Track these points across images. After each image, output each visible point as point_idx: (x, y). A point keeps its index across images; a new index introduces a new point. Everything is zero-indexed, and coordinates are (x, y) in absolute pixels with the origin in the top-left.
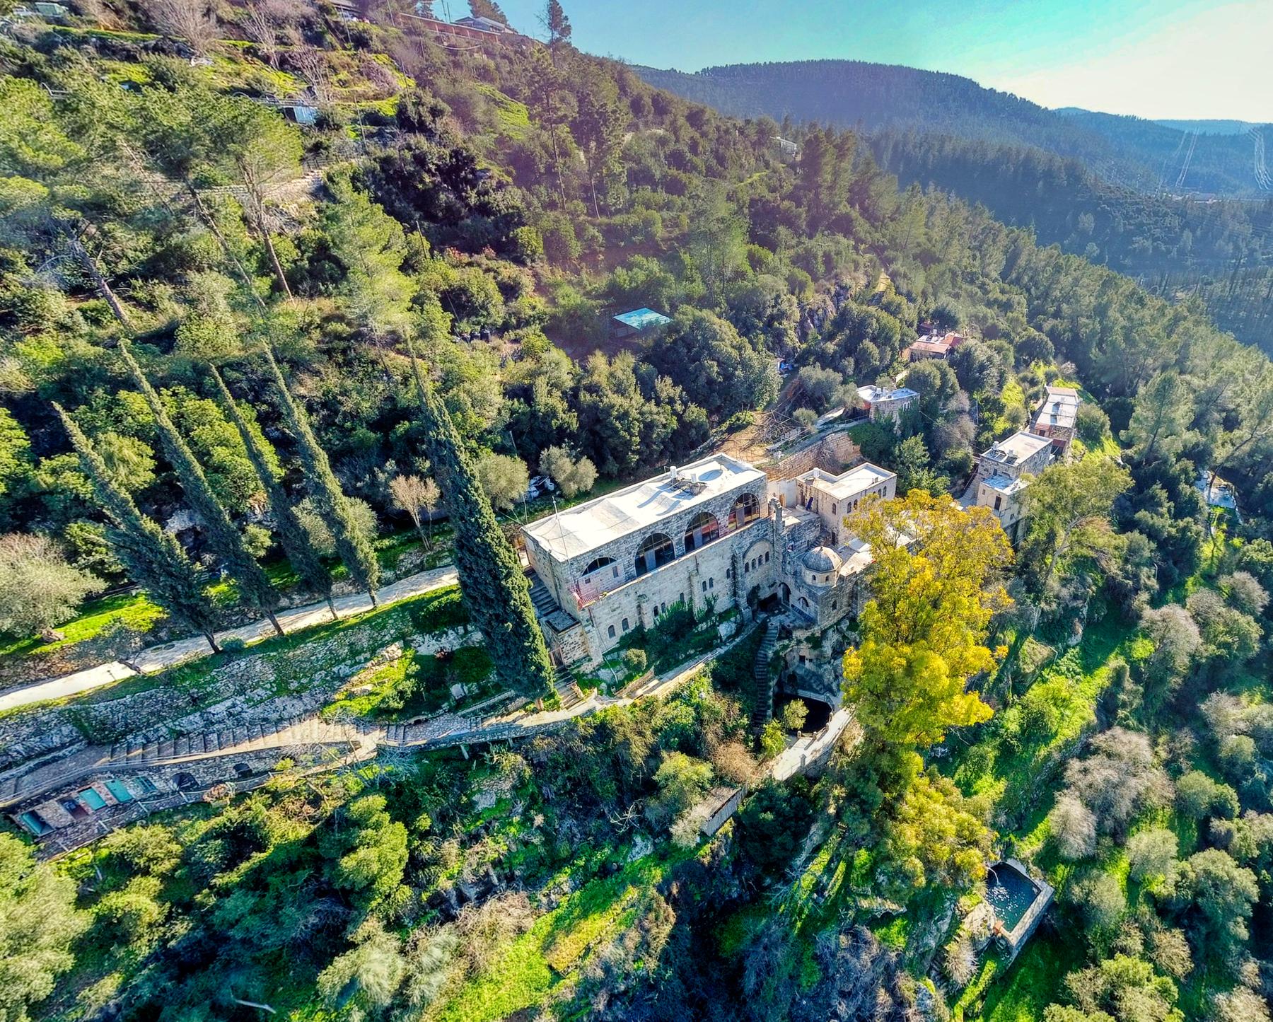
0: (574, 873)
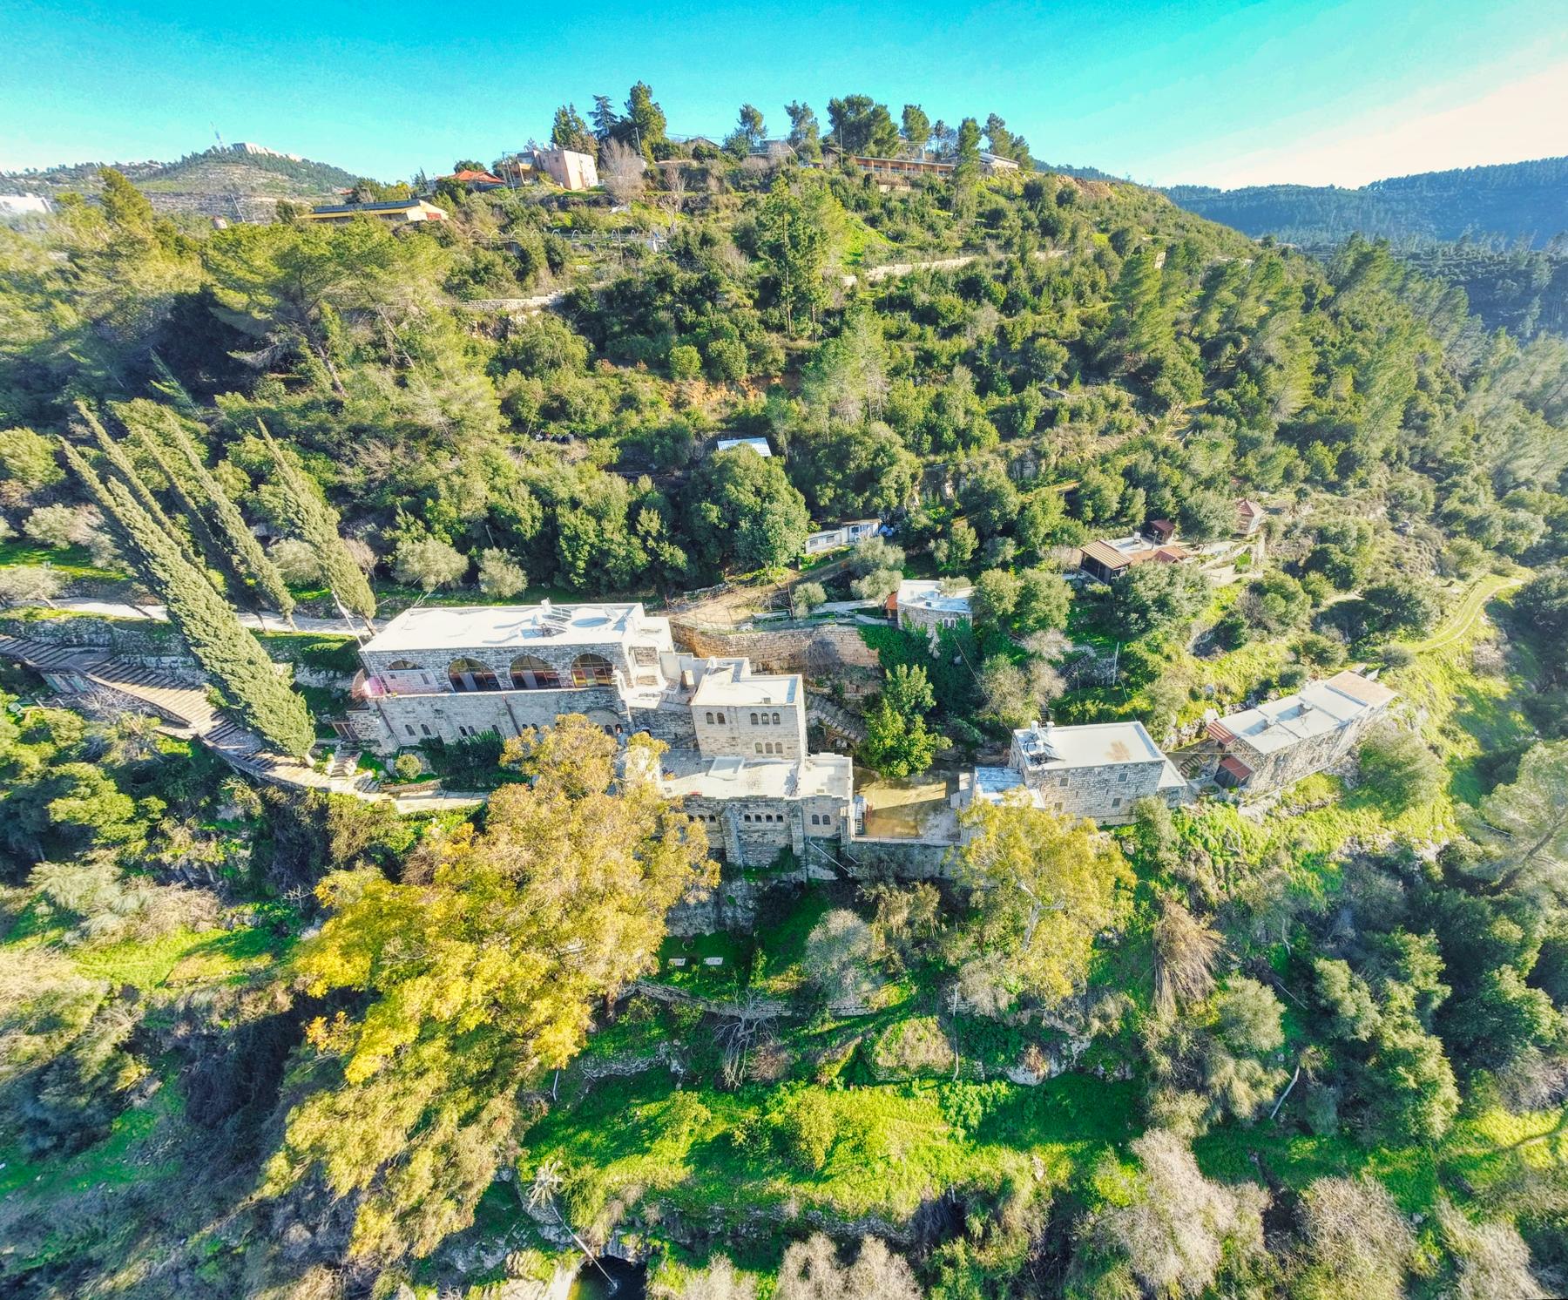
0: (259, 912)
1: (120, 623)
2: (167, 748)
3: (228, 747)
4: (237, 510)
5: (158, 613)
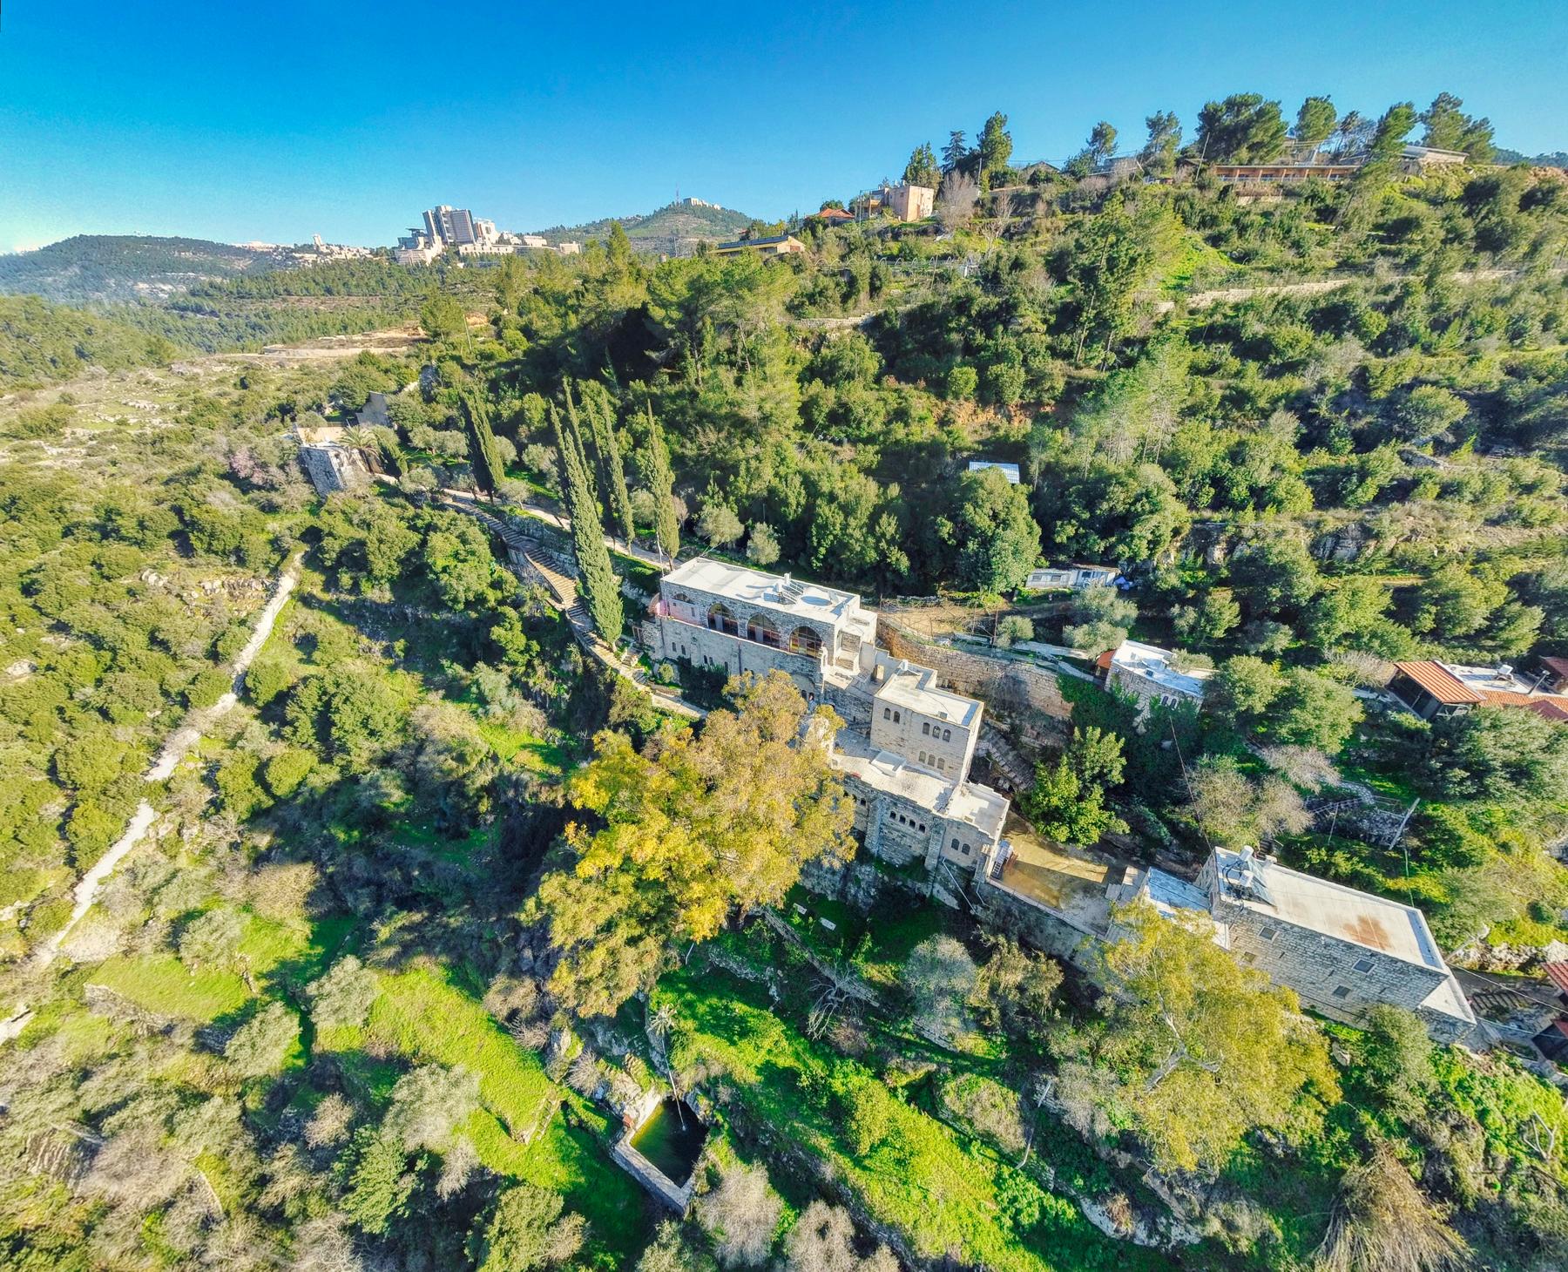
1: (549, 526)
2: (549, 612)
3: (576, 623)
4: (621, 463)
5: (565, 524)
